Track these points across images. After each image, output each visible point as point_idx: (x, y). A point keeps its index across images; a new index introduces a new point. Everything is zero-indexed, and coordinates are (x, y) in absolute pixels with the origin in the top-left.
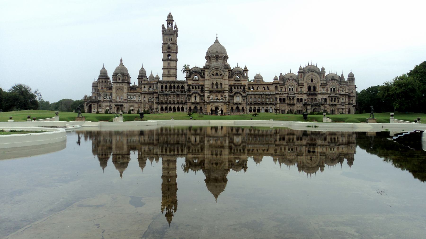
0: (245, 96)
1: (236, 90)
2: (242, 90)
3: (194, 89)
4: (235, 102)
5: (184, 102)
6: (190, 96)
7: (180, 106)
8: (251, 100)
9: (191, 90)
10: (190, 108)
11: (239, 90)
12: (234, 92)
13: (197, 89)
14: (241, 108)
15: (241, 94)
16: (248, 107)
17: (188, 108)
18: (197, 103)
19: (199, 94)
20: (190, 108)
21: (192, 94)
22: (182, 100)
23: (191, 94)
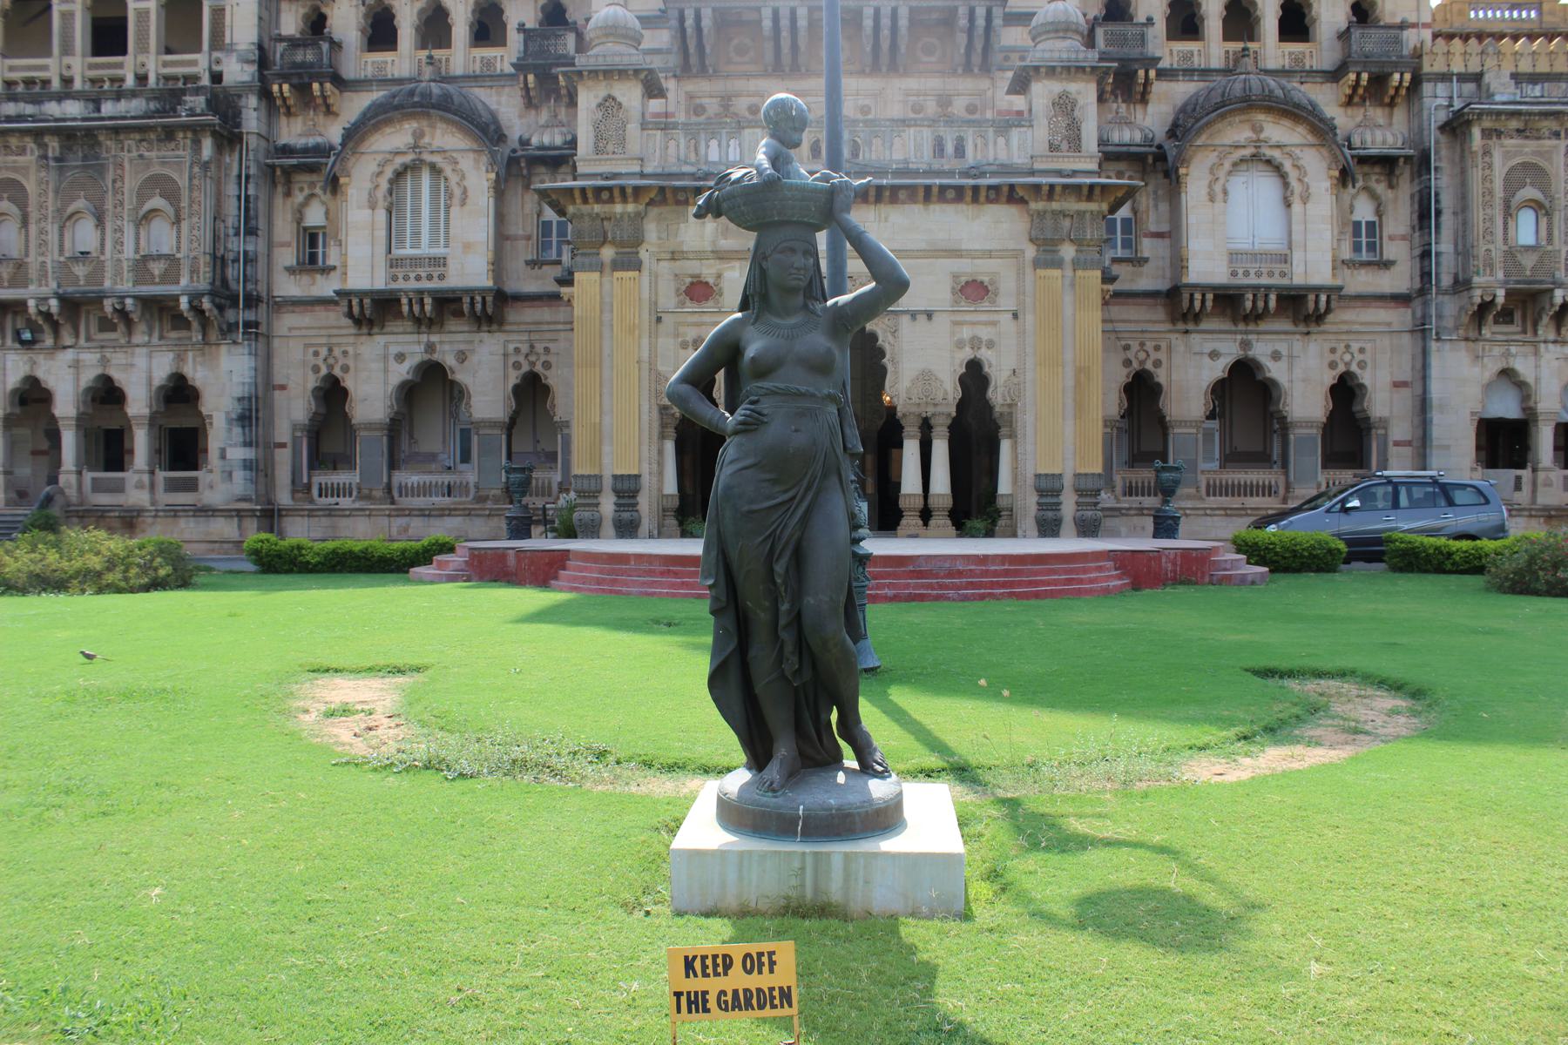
0: (1386, 164)
1: (1214, 48)
2: (1321, 51)
3: (404, 59)
4: (1207, 265)
5: (185, 286)
6: (319, 168)
7: (142, 371)
8: (1526, 229)
9: (357, 62)
10: (332, 394)
11: (1272, 49)
12: (1167, 99)
13: (461, 55)
14: (1306, 402)
15: (1321, 129)
16: (1464, 383)
17: (294, 408)
18: (448, 306)
19: (487, 132)
20: (332, 394)
21: (355, 134)
22: (162, 237)
23: (334, 133)
